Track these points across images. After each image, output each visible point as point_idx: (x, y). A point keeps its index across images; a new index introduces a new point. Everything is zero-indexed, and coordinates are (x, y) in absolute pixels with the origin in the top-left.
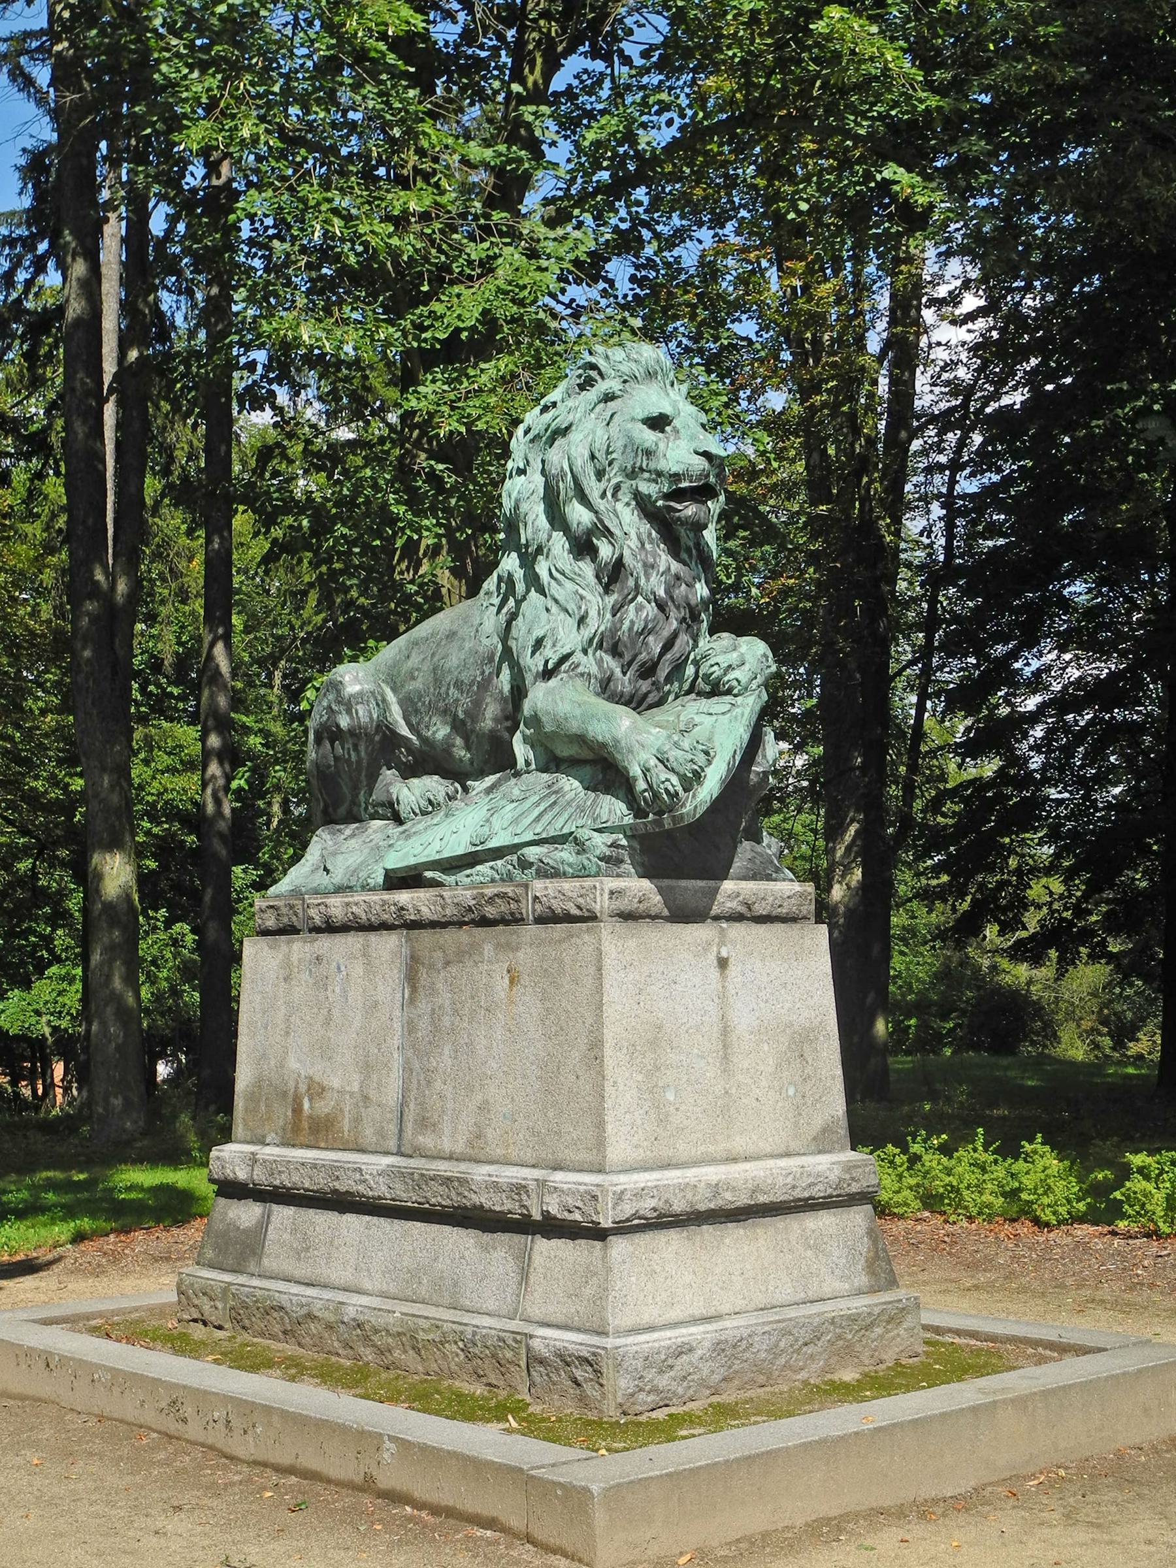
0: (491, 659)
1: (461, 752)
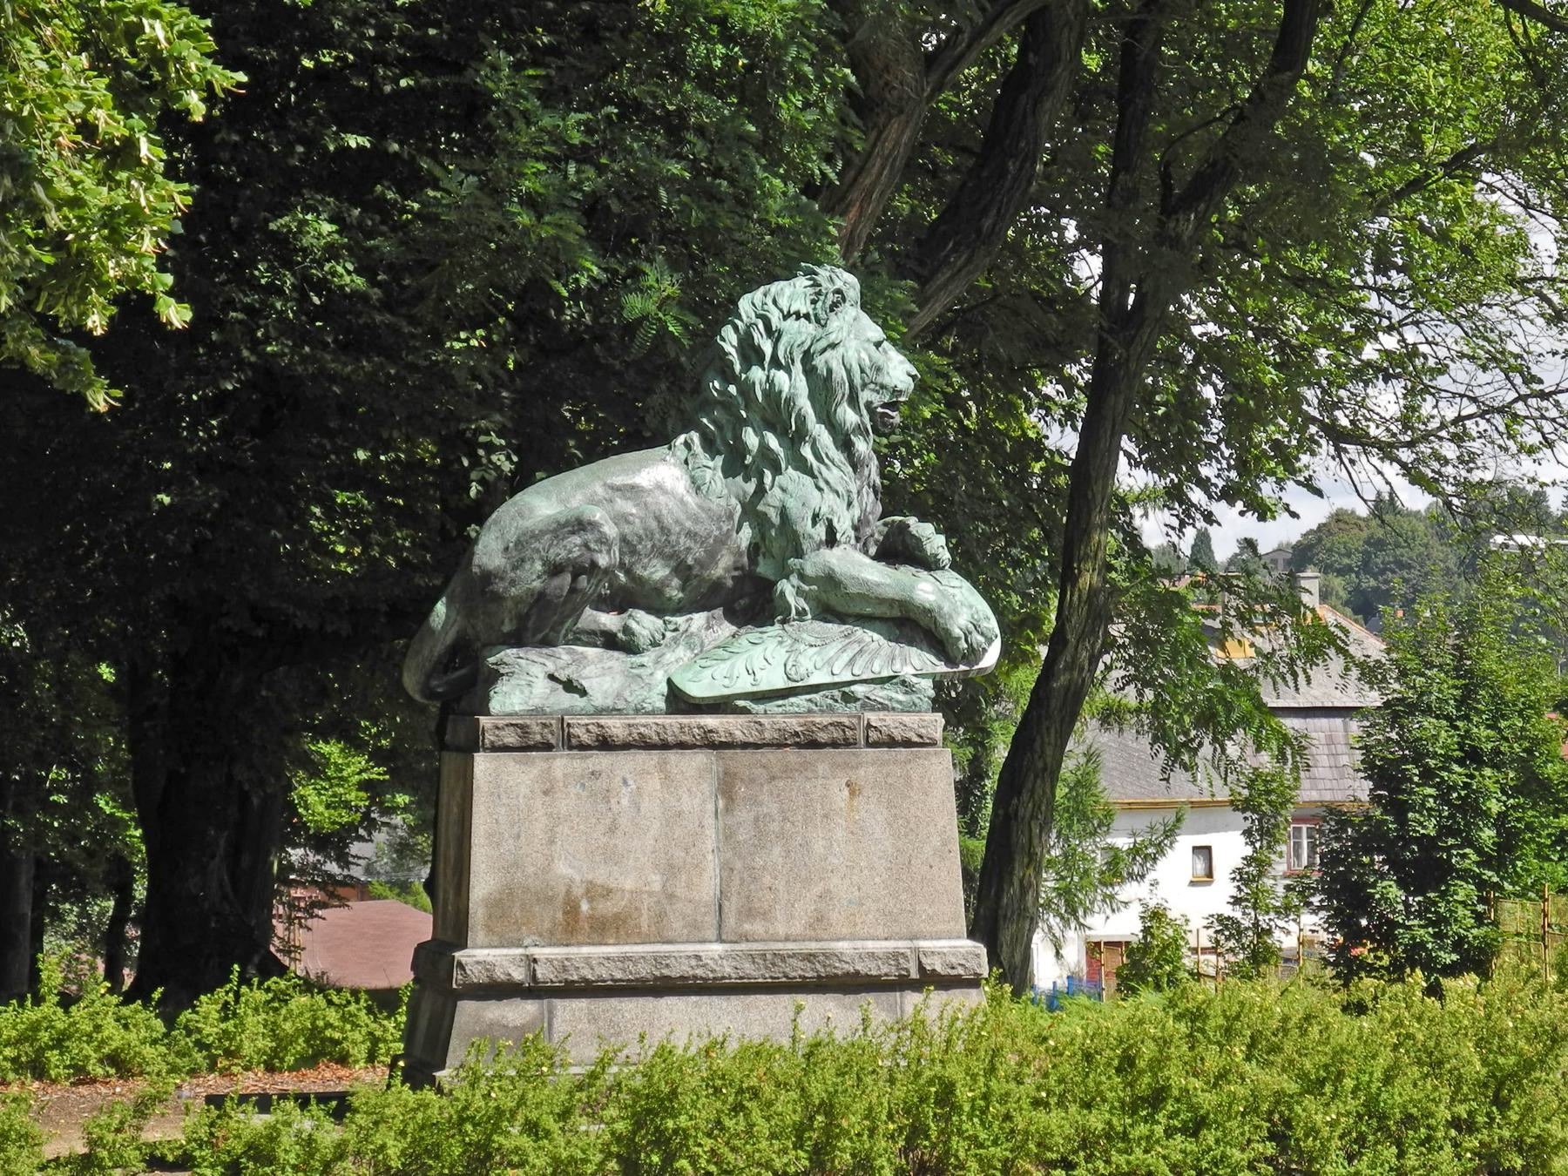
0: (730, 516)
1: (674, 592)
